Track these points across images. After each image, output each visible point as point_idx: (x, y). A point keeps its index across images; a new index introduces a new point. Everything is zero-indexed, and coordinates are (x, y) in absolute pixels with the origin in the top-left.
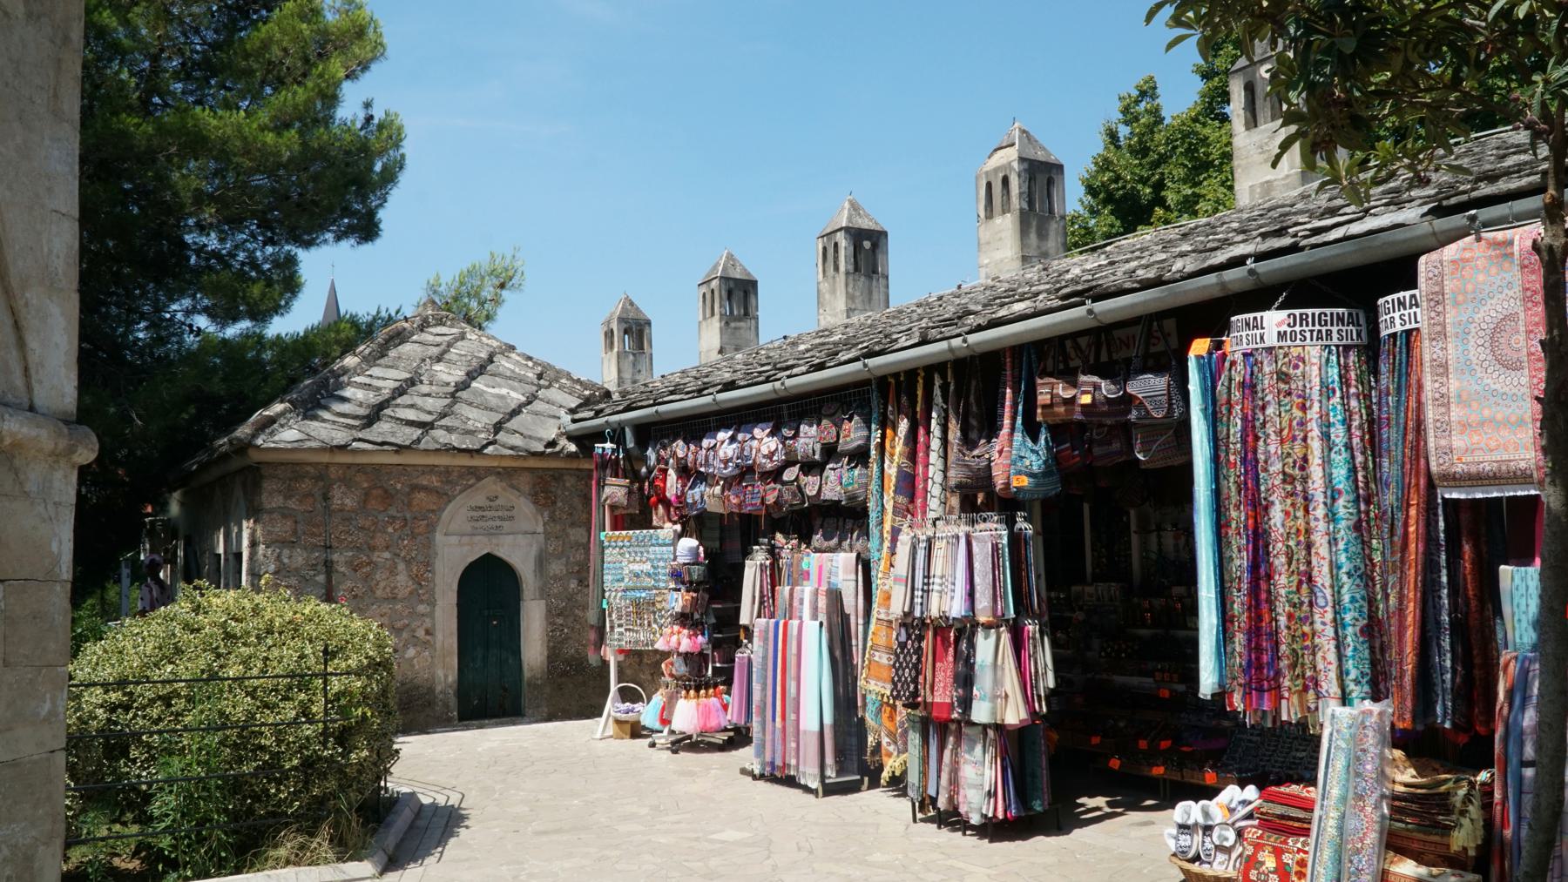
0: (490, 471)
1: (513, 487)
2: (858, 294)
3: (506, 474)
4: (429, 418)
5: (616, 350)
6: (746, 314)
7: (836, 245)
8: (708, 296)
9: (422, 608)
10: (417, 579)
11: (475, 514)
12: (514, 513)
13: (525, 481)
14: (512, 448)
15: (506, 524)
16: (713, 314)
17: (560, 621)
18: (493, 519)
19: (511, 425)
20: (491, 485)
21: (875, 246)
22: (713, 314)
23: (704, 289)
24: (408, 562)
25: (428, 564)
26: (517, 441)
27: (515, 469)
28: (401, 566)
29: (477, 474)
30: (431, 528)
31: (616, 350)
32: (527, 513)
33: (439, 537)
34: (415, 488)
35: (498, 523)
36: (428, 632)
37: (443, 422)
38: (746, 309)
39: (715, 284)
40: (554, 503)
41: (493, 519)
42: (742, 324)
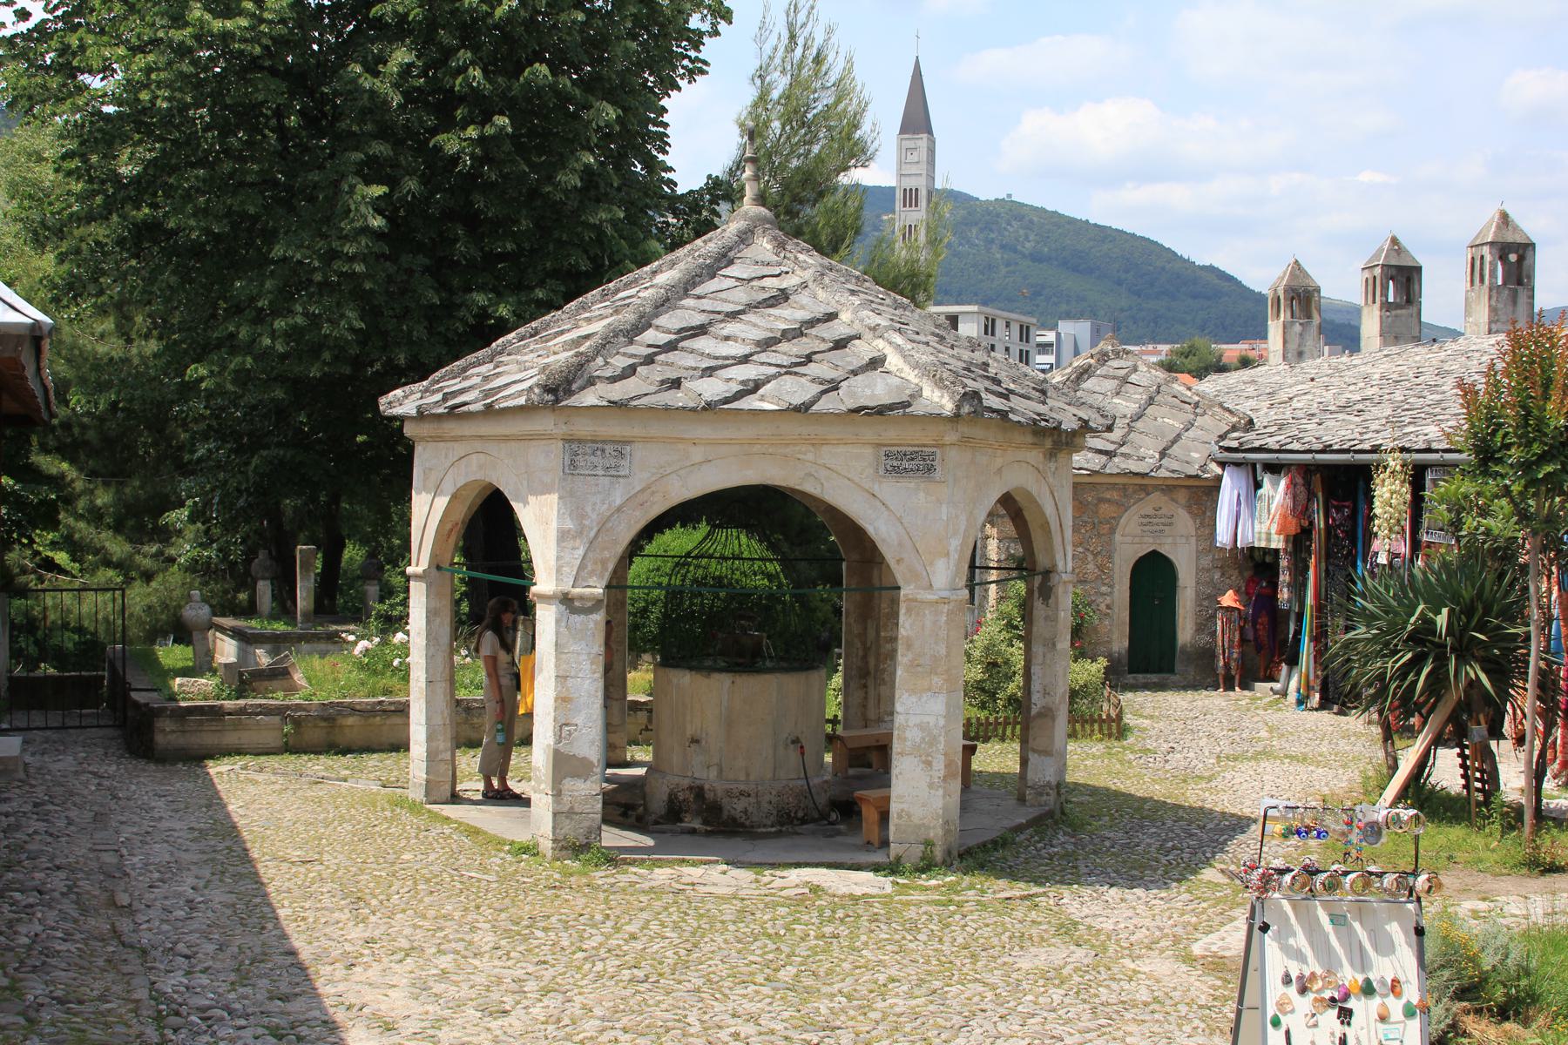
0: (1156, 488)
1: (1173, 500)
2: (1500, 306)
3: (1169, 488)
4: (1111, 447)
5: (1282, 319)
6: (1409, 301)
7: (1482, 257)
8: (1371, 282)
9: (1104, 589)
10: (1101, 568)
11: (1145, 521)
12: (1173, 520)
13: (1182, 496)
14: (1173, 471)
15: (1166, 528)
16: (1374, 302)
17: (1206, 603)
18: (1157, 524)
19: (1175, 450)
20: (1157, 498)
21: (1521, 259)
22: (1374, 302)
23: (1367, 274)
24: (1095, 555)
25: (1110, 557)
26: (1175, 465)
27: (1175, 487)
28: (1090, 557)
29: (1145, 490)
30: (1112, 531)
31: (1282, 319)
32: (1184, 522)
33: (1118, 537)
34: (1101, 500)
35: (1162, 527)
36: (1108, 607)
37: (1123, 450)
38: (1408, 295)
39: (1378, 271)
40: (1204, 513)
41: (1157, 524)
42: (1403, 311)
